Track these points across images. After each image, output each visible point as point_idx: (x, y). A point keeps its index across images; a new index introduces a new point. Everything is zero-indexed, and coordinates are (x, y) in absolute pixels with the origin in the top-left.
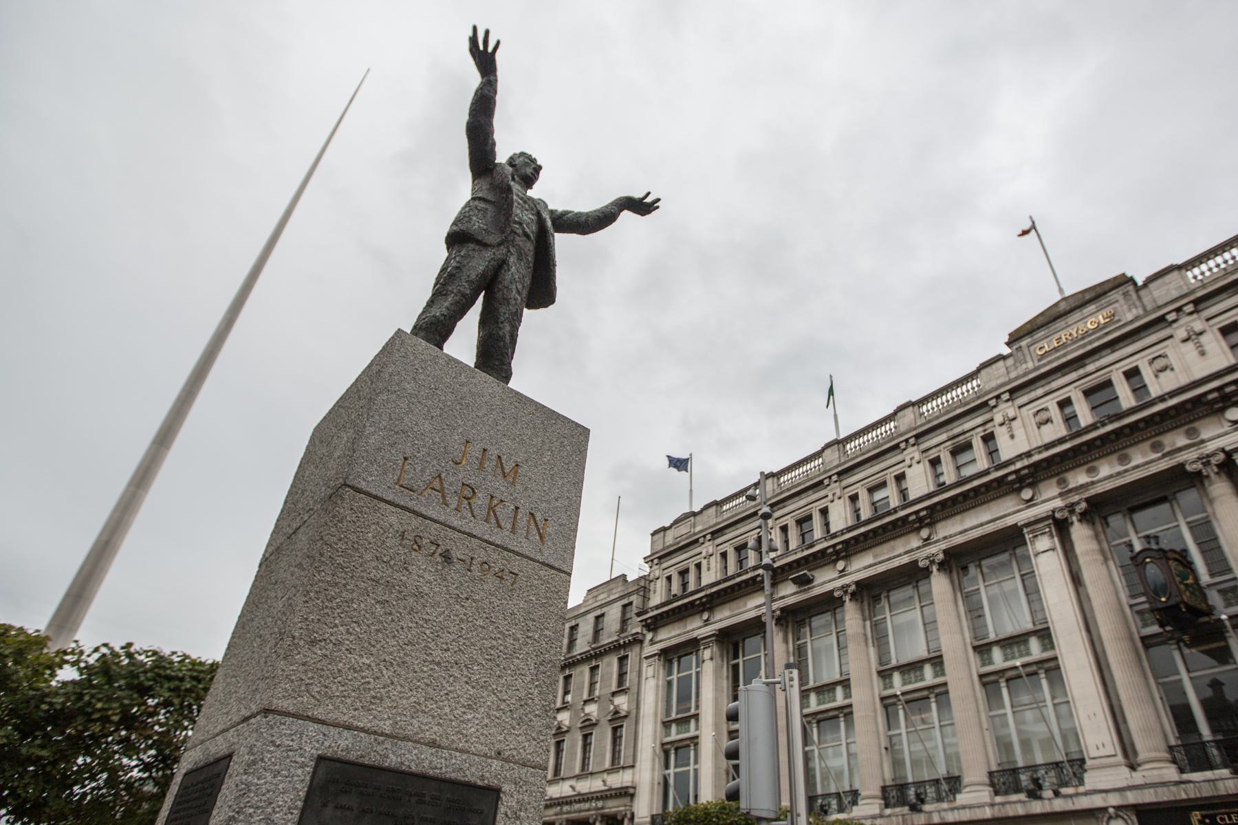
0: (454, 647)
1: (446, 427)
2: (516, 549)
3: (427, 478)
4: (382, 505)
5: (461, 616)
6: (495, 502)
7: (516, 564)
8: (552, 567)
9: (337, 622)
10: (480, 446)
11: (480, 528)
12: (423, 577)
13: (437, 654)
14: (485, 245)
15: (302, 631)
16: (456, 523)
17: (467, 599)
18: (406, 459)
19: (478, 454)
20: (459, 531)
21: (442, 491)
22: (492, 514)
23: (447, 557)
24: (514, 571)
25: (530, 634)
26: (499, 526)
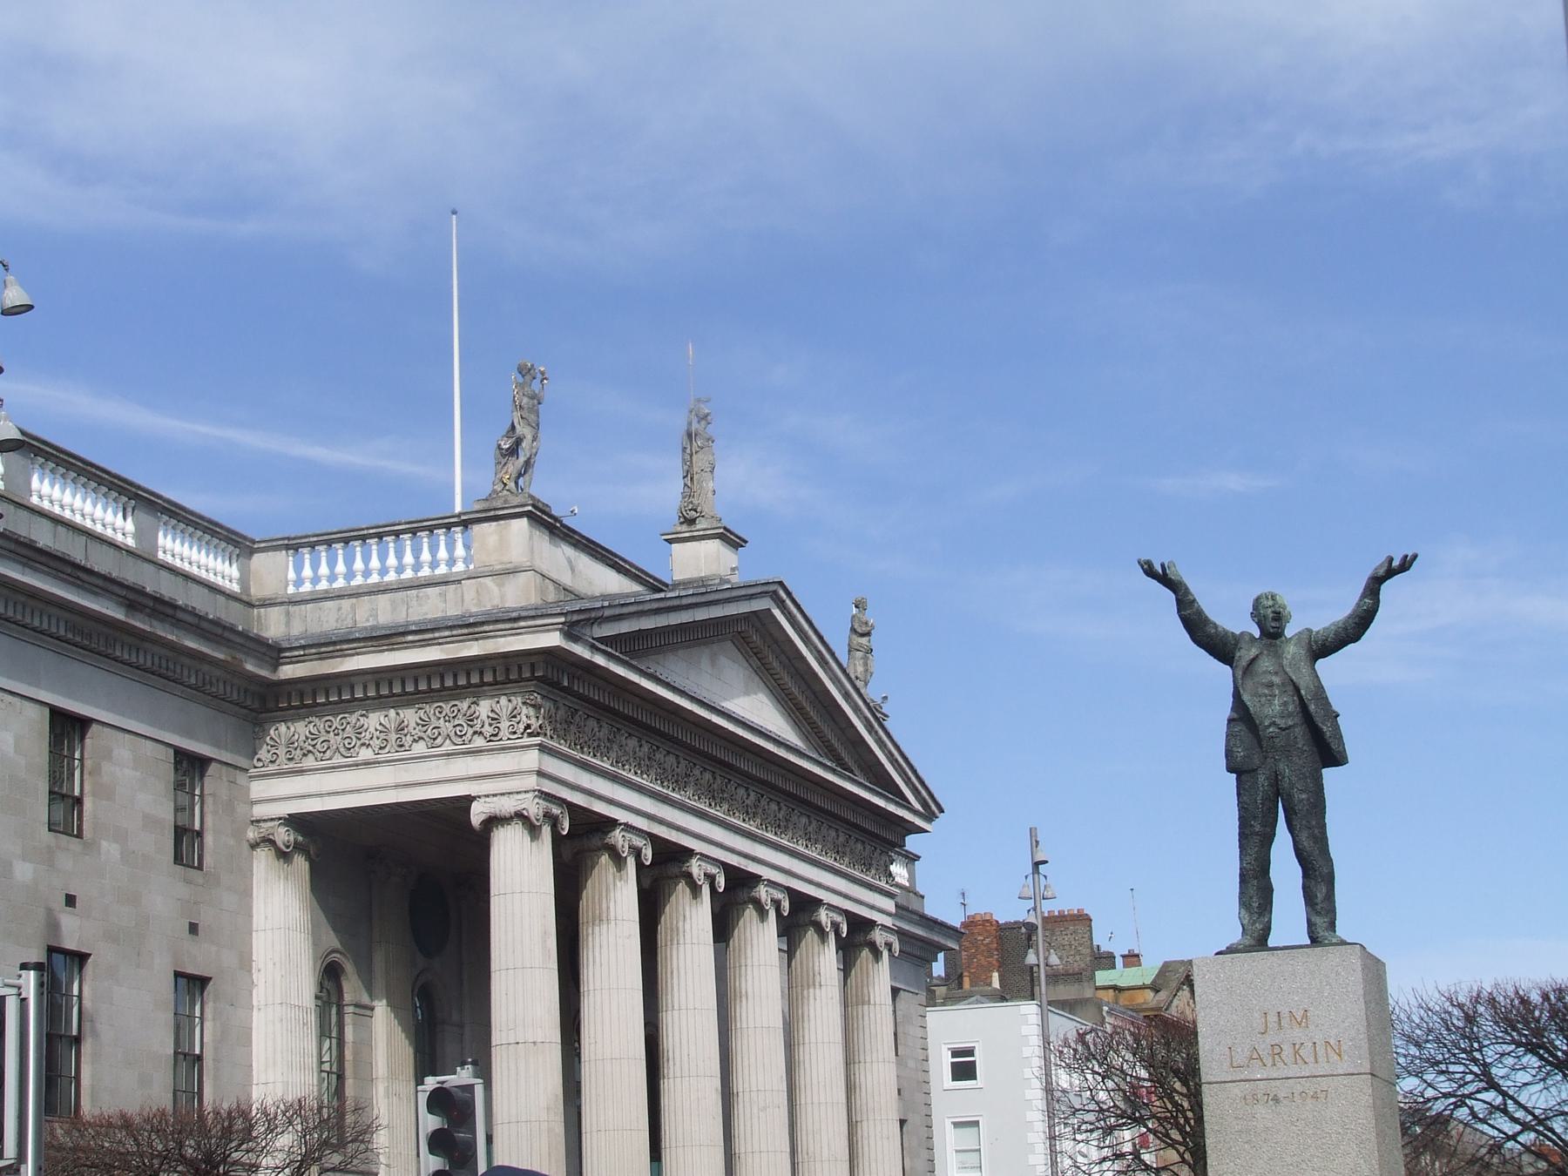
2: (1321, 1073)
6: (1297, 1047)
7: (1324, 1083)
11: (1293, 1071)
13: (1289, 1160)
16: (1275, 1076)
18: (1230, 1048)
19: (1276, 1019)
22: (1298, 1056)
23: (1276, 1100)
26: (1306, 1063)
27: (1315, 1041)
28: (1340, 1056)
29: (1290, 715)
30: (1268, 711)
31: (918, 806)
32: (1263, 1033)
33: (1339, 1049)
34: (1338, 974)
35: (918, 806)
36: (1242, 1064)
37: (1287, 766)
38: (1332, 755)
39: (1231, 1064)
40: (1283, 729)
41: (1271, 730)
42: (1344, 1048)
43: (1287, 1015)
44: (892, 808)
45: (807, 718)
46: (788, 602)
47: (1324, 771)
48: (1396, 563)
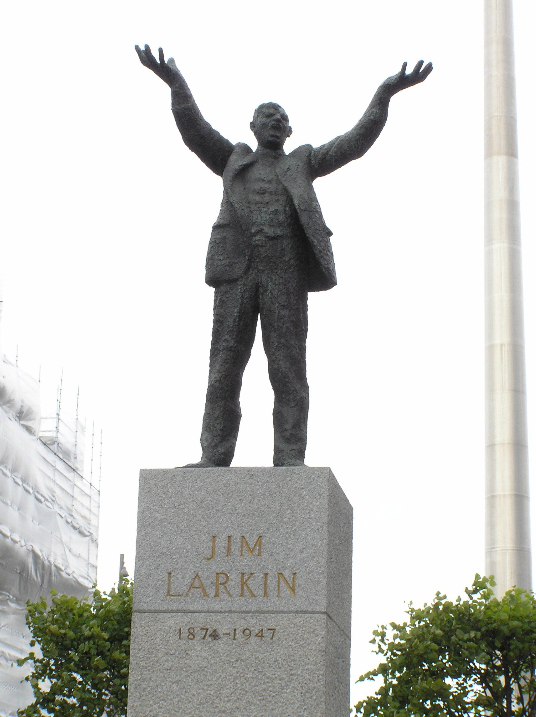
0: (234, 697)
1: (194, 533)
2: (271, 609)
3: (188, 581)
4: (161, 615)
5: (234, 675)
6: (246, 577)
7: (272, 621)
8: (305, 612)
9: (151, 703)
10: (224, 537)
11: (238, 603)
12: (201, 656)
14: (235, 281)
15: (132, 714)
17: (237, 661)
18: (170, 573)
19: (225, 544)
20: (221, 612)
23: (215, 636)
24: (271, 628)
25: (293, 672)
26: (254, 596)
27: (266, 571)
28: (293, 590)
29: (280, 225)
30: (256, 217)
32: (209, 559)
33: (294, 582)
34: (302, 497)
36: (181, 592)
37: (272, 279)
39: (169, 592)
41: (257, 238)
42: (299, 581)
47: (309, 293)
48: (409, 71)
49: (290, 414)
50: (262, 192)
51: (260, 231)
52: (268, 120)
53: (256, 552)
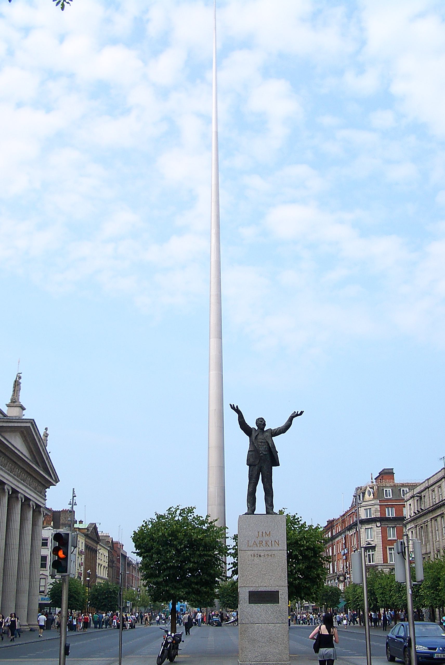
3: (253, 543)
4: (246, 551)
6: (267, 542)
10: (261, 532)
14: (256, 465)
21: (256, 544)
22: (267, 545)
23: (260, 556)
28: (278, 545)
29: (266, 451)
31: (54, 479)
35: (54, 479)
38: (277, 464)
40: (264, 455)
41: (261, 454)
43: (265, 533)
44: (49, 479)
45: (33, 454)
46: (34, 425)
48: (299, 413)
49: (269, 499)
50: (261, 442)
51: (262, 453)
52: (261, 423)
53: (269, 536)
